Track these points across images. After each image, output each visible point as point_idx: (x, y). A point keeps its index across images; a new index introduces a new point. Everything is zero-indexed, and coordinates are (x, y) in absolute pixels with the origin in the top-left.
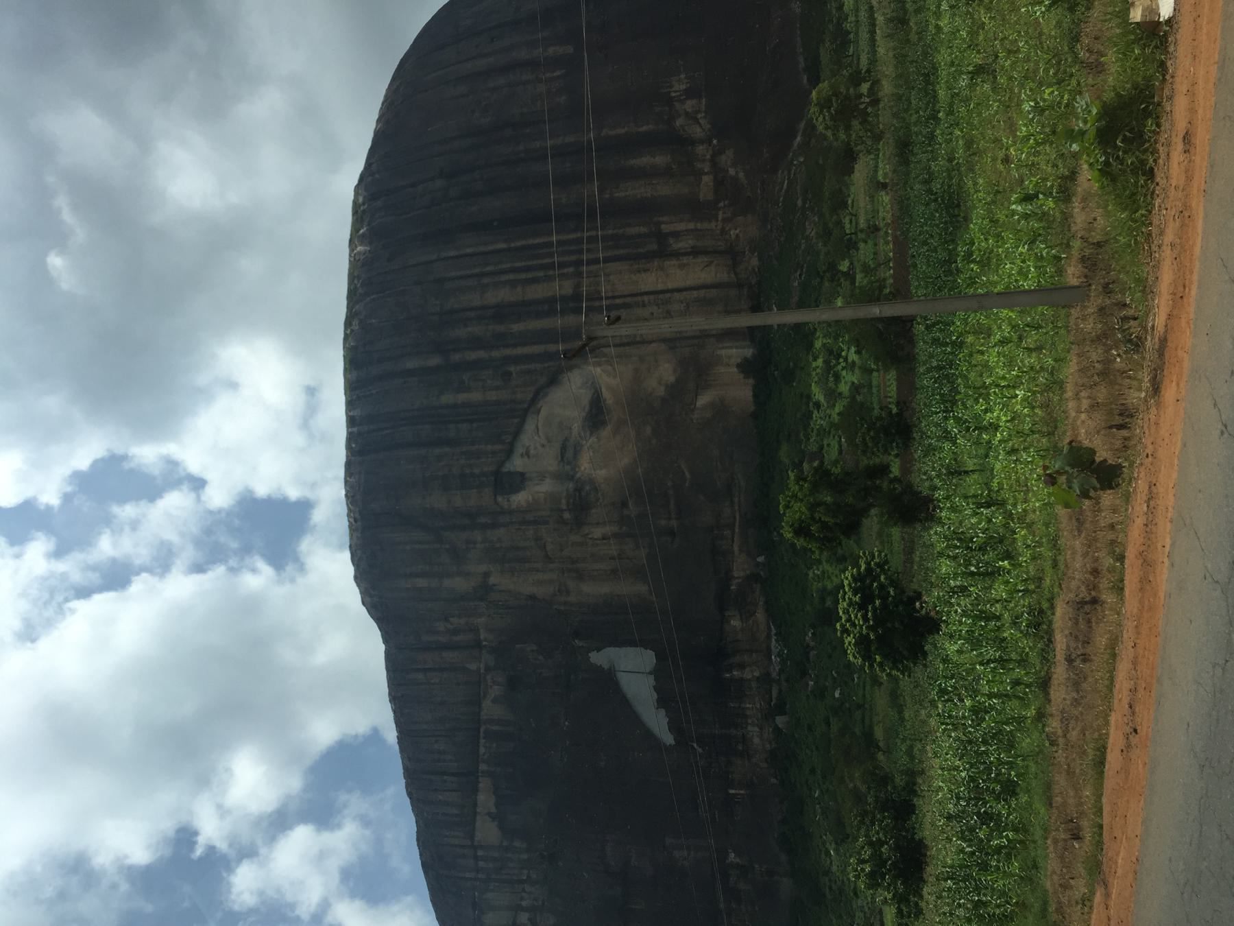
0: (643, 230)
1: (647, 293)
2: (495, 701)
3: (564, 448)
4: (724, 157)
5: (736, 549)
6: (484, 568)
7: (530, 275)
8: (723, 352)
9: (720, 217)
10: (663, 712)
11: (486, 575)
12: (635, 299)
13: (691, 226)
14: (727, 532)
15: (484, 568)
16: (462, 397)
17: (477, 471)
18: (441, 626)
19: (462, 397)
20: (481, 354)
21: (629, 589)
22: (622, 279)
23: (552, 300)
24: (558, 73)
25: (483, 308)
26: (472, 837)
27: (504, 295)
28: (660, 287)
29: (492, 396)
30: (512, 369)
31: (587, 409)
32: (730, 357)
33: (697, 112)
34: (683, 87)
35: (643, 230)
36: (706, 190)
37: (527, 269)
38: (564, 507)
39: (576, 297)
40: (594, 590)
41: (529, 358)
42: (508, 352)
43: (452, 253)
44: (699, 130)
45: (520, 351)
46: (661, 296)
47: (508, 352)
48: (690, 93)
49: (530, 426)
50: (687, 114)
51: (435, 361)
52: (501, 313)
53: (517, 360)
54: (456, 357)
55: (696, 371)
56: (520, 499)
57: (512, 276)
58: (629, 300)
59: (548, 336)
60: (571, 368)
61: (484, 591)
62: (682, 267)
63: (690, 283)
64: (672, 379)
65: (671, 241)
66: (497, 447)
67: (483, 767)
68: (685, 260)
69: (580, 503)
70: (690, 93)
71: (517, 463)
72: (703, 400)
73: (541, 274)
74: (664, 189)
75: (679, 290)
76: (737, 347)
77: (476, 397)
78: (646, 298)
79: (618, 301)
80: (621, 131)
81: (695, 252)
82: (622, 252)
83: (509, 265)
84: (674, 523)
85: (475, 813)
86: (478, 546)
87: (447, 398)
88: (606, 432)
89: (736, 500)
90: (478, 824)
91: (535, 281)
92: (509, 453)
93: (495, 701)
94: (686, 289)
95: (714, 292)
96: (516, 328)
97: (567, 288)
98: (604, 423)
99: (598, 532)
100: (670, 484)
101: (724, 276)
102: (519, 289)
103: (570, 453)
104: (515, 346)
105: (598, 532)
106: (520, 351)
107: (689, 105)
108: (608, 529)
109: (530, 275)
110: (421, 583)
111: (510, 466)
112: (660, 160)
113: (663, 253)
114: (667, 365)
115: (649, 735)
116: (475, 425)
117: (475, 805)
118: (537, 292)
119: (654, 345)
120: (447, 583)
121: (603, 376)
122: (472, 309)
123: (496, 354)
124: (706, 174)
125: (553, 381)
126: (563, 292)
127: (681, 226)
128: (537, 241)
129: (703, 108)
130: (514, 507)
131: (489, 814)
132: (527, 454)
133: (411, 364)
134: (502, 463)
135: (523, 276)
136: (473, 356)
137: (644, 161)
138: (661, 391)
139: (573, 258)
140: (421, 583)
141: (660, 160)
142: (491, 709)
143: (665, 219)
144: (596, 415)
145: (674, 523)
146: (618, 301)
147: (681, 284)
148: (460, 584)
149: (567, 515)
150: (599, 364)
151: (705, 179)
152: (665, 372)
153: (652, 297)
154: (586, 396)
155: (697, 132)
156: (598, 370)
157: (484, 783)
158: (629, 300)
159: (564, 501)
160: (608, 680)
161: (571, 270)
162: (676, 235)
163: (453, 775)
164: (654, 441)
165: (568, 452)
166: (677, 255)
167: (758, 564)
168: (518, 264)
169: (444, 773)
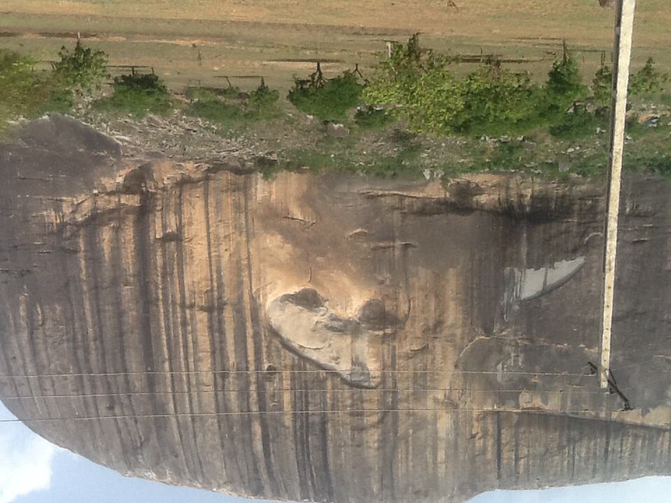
0: (159, 253)
1: (210, 253)
2: (545, 401)
3: (332, 329)
4: (107, 185)
5: (421, 195)
6: (430, 403)
7: (191, 345)
8: (260, 196)
9: (153, 191)
10: (556, 264)
11: (436, 400)
12: (213, 262)
13: (158, 214)
14: (407, 201)
15: (430, 403)
16: (287, 407)
17: (349, 402)
18: (479, 444)
19: (287, 407)
20: (253, 387)
21: (452, 283)
22: (196, 274)
23: (211, 328)
24: (39, 309)
25: (215, 385)
26: (660, 431)
27: (206, 365)
28: (205, 242)
29: (287, 384)
30: (266, 366)
31: (300, 307)
32: (264, 190)
33: (73, 204)
34: (53, 213)
35: (159, 253)
36: (133, 201)
37: (186, 347)
38: (381, 333)
39: (209, 309)
40: (453, 315)
41: (258, 352)
42: (252, 368)
43: (171, 405)
44: (86, 204)
45: (251, 358)
46: (212, 242)
47: (252, 368)
48: (58, 209)
49: (314, 356)
50: (73, 212)
51: (257, 428)
52: (221, 375)
54: (255, 408)
55: (274, 218)
56: (373, 367)
57: (191, 360)
58: (214, 268)
60: (268, 319)
61: (451, 405)
62: (190, 224)
63: (203, 219)
64: (279, 237)
65: (169, 231)
66: (329, 383)
67: (603, 415)
68: (185, 221)
69: (380, 319)
70: (58, 209)
72: (297, 213)
73: (190, 337)
74: (129, 233)
75: (208, 228)
76: (257, 184)
77: (287, 397)
78: (213, 254)
79: (215, 277)
80: (83, 262)
81: (179, 212)
82: (176, 271)
83: (182, 360)
84: (398, 243)
85: (643, 427)
86: (411, 406)
87: (288, 420)
88: (321, 293)
89: (380, 193)
90: (651, 424)
91: (195, 342)
92: (335, 374)
93: (545, 401)
94: (208, 222)
95: (211, 200)
96: (232, 359)
97: (202, 317)
98: (315, 294)
99: (404, 308)
100: (365, 245)
101: (199, 192)
102: (201, 355)
103: (335, 324)
104: (247, 362)
106: (251, 358)
107: (67, 209)
109: (191, 345)
110: (441, 455)
111: (346, 375)
113: (176, 238)
114: (268, 241)
115: (575, 276)
116: (310, 400)
117: (635, 426)
118: (204, 340)
119: (251, 250)
120: (442, 434)
121: (274, 293)
122: (216, 395)
123: (253, 379)
124: (119, 200)
125: (275, 333)
126: (206, 320)
127: (158, 221)
128: (164, 337)
129: (69, 199)
130: (378, 373)
131: (643, 414)
132: (336, 359)
133: (259, 446)
134: (344, 381)
135: (191, 350)
136: (254, 395)
137: (106, 247)
138: (288, 247)
139: (178, 309)
140: (441, 455)
141: (106, 234)
143: (151, 234)
144: (309, 300)
145: (398, 243)
146: (215, 277)
147: (203, 226)
148: (445, 424)
149: (389, 331)
150: (265, 295)
151: (123, 201)
152: (273, 243)
153: (212, 249)
154: (293, 308)
155: (87, 206)
156: (269, 296)
158: (214, 268)
159: (377, 333)
161: (188, 311)
162: (164, 227)
163: (607, 443)
164: (330, 255)
166: (180, 227)
167: (432, 178)
168: (182, 354)
169: (606, 451)
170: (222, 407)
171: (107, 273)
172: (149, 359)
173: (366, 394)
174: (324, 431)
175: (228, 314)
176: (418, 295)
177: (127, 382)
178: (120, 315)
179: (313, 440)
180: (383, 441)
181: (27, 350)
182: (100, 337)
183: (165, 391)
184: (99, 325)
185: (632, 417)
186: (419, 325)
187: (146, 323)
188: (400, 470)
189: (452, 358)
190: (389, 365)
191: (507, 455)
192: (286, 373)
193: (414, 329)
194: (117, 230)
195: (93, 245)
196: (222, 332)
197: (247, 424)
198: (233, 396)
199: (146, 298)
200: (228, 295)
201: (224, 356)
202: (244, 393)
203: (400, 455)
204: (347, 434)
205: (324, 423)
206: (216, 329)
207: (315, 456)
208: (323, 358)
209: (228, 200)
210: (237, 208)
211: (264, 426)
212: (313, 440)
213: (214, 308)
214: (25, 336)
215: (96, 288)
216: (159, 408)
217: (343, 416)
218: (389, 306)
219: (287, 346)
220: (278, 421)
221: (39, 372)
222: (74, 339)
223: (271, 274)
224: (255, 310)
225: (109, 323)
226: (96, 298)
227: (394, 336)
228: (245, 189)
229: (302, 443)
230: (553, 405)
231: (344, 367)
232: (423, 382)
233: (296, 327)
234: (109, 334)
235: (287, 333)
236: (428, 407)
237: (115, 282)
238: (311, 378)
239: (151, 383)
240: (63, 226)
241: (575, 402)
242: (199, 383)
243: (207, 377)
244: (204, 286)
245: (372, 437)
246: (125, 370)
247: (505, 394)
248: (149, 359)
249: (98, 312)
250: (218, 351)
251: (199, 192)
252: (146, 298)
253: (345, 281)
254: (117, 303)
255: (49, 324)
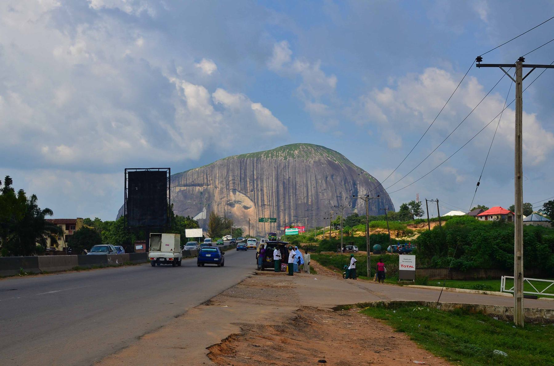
16: (248, 183)
19: (248, 183)
27: (265, 191)
29: (248, 189)
39: (264, 205)
49: (243, 195)
51: (255, 177)
52: (262, 190)
53: (254, 193)
56: (231, 194)
59: (258, 199)
69: (231, 205)
71: (237, 193)
77: (248, 185)
81: (271, 227)
87: (248, 180)
88: (243, 209)
92: (239, 192)
96: (260, 193)
97: (266, 203)
101: (266, 231)
105: (226, 208)
108: (226, 210)
112: (287, 221)
125: (251, 200)
133: (255, 173)
137: (287, 218)
142: (197, 188)
144: (246, 208)
148: (217, 182)
157: (186, 188)
160: (200, 210)
165: (239, 202)
170: (262, 181)
171: (287, 212)
172: (278, 192)
173: (232, 188)
174: (241, 178)
175: (260, 204)
176: (223, 211)
177: (284, 186)
178: (284, 202)
179: (243, 176)
180: (229, 178)
181: (309, 190)
182: (289, 196)
183: (275, 184)
184: (289, 199)
185: (183, 188)
186: (222, 204)
187: (278, 201)
188: (225, 171)
189: (215, 198)
190: (228, 194)
191: (205, 177)
192: (248, 191)
193: (223, 203)
194: (285, 222)
195: (290, 218)
196: (261, 200)
197: (257, 178)
198: (259, 186)
199: (278, 206)
200: (260, 208)
201: (261, 194)
202: (257, 185)
203: (225, 174)
204: (236, 179)
205: (240, 181)
206: (263, 200)
207: (243, 172)
208: (242, 195)
209: (260, 230)
210: (259, 228)
211: (254, 178)
212: (243, 176)
213: (263, 205)
214: (310, 194)
215: (289, 208)
216: (277, 179)
217: (237, 182)
218: (229, 207)
219: (249, 198)
220: (250, 180)
221: (307, 184)
222: (296, 195)
223: (252, 214)
224: (255, 205)
225: (287, 200)
226: (289, 206)
227: (228, 201)
228: (257, 232)
229: (245, 175)
230: (197, 188)
231: (237, 193)
232: (221, 192)
233: (248, 202)
234: (287, 197)
235: (249, 200)
236: (220, 186)
237: (285, 210)
238: (244, 191)
239: (278, 186)
240: (297, 222)
241: (193, 190)
242: (266, 187)
243: (265, 189)
244: (266, 210)
245: (231, 178)
246: (284, 188)
247: (205, 190)
248: (278, 192)
249: (289, 202)
250: (263, 195)
251: (266, 231)
252: (278, 206)
253: (237, 213)
254: (284, 205)
255: (302, 198)
